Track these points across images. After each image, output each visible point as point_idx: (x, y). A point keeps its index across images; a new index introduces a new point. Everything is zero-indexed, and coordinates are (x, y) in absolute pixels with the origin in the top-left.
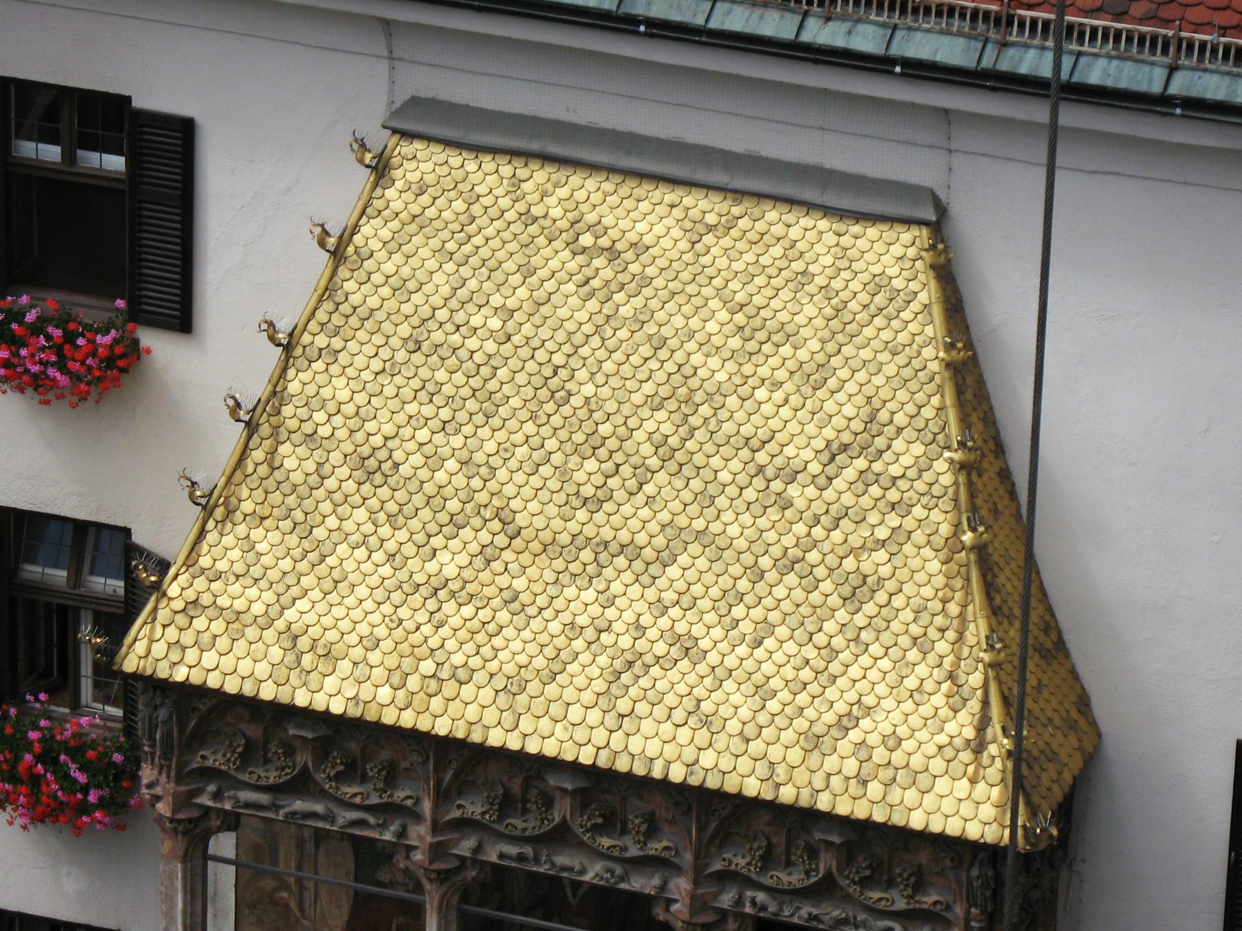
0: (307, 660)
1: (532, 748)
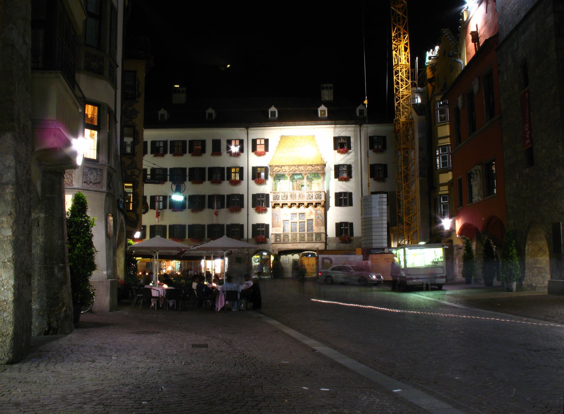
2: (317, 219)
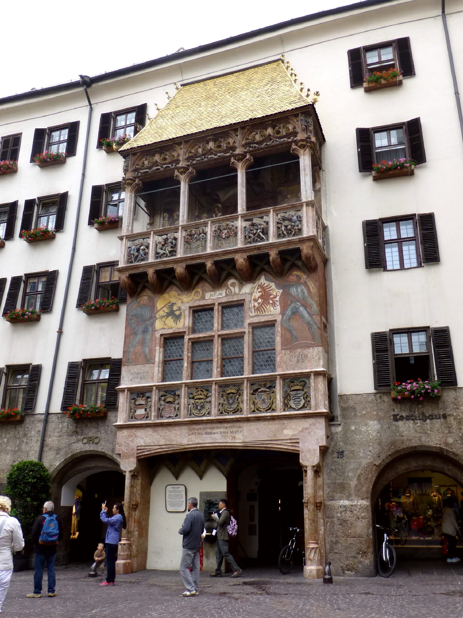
2: (290, 319)
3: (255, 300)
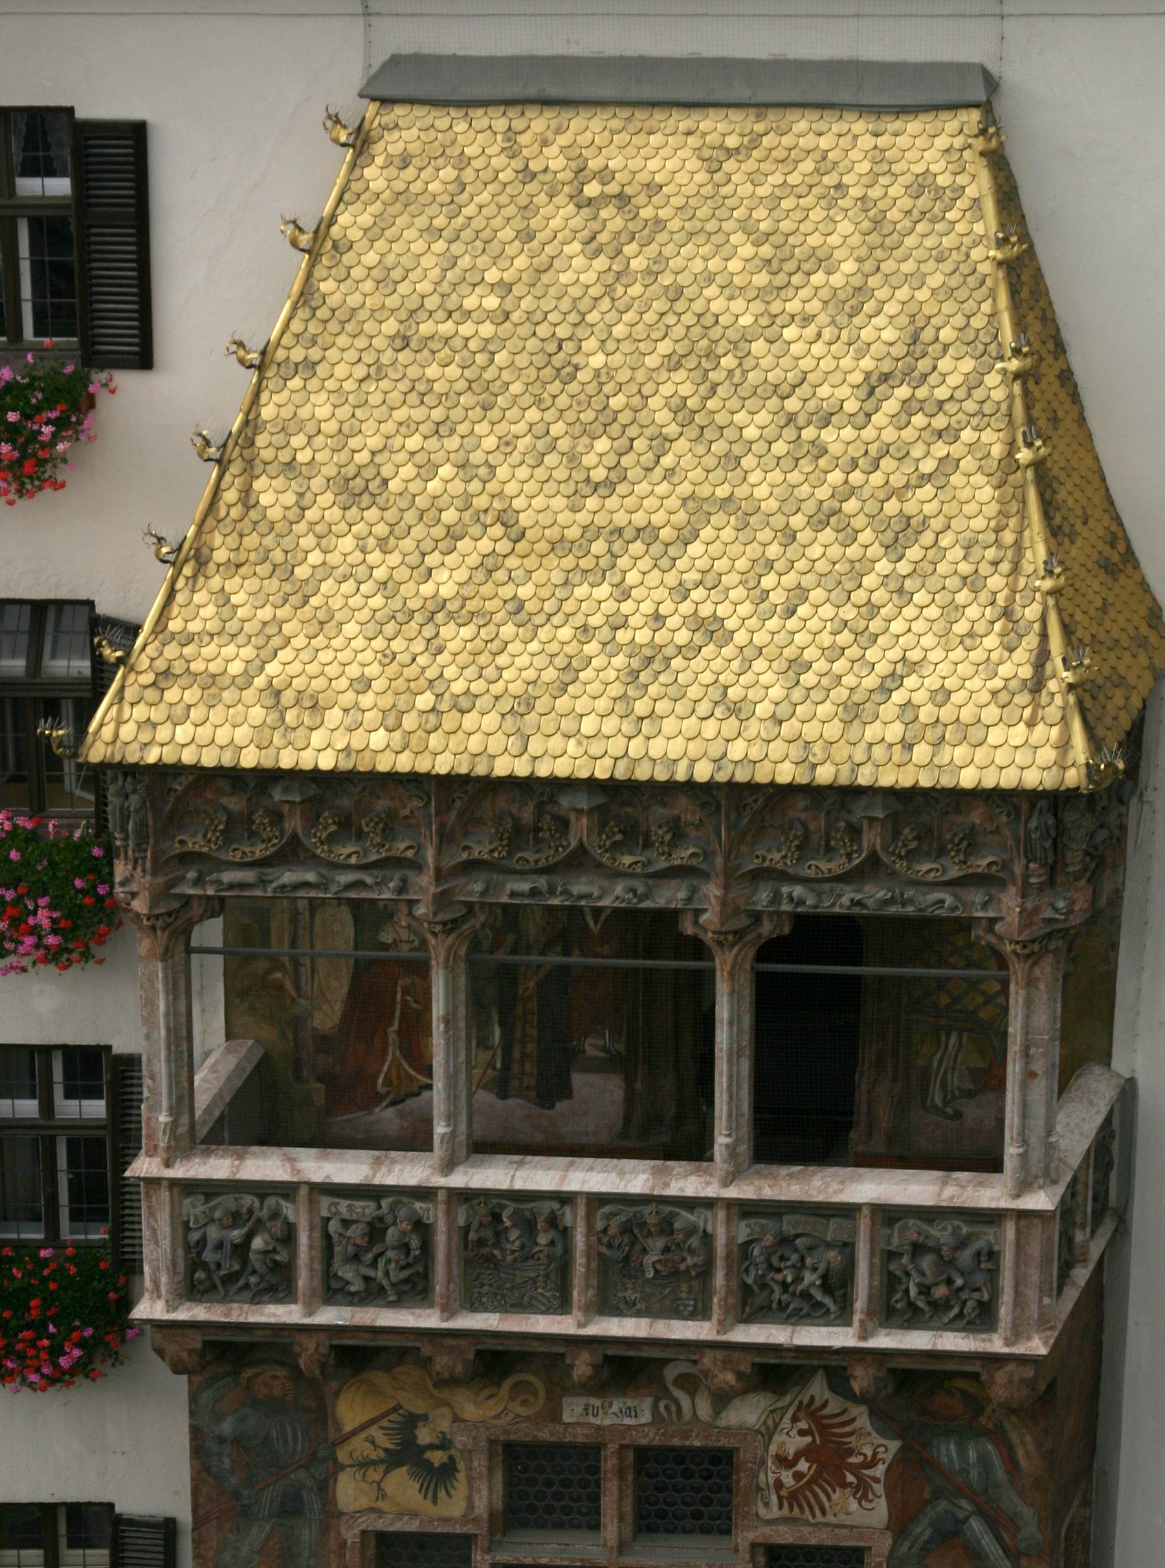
0: (290, 717)
1: (543, 771)
2: (925, 1551)
3: (784, 1462)
